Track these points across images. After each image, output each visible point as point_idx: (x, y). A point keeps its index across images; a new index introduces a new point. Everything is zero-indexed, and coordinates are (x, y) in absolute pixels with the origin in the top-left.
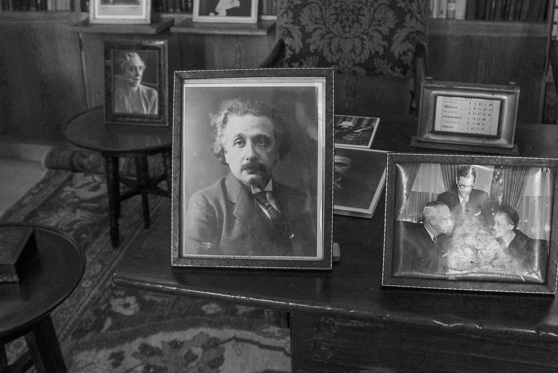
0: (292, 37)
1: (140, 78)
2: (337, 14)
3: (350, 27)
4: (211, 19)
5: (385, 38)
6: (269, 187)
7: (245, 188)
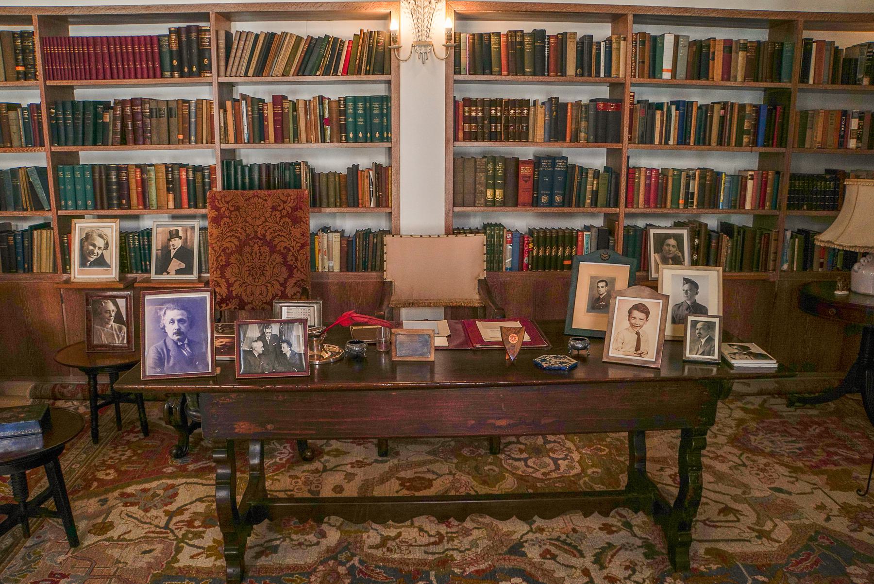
0: (220, 286)
1: (112, 318)
2: (249, 270)
3: (258, 279)
4: (164, 277)
5: (281, 285)
6: (186, 342)
7: (175, 343)
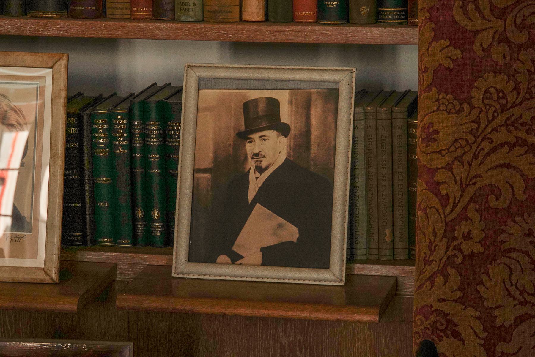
0: (456, 335)
